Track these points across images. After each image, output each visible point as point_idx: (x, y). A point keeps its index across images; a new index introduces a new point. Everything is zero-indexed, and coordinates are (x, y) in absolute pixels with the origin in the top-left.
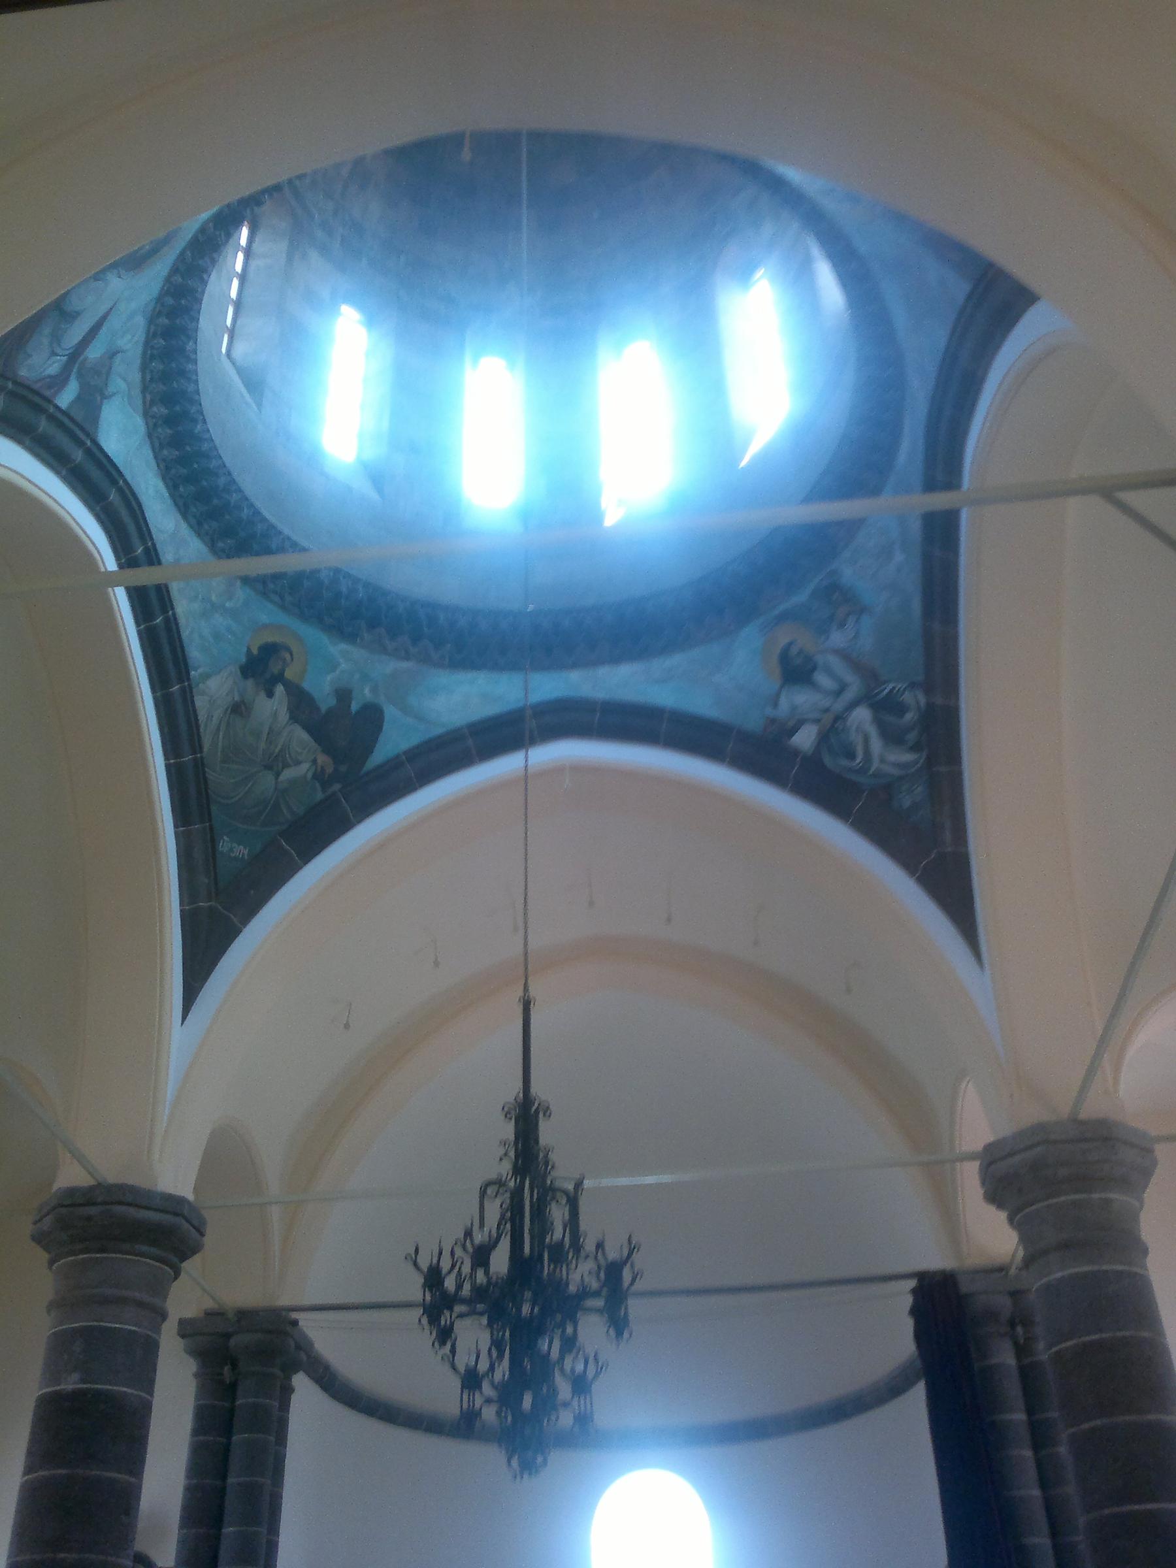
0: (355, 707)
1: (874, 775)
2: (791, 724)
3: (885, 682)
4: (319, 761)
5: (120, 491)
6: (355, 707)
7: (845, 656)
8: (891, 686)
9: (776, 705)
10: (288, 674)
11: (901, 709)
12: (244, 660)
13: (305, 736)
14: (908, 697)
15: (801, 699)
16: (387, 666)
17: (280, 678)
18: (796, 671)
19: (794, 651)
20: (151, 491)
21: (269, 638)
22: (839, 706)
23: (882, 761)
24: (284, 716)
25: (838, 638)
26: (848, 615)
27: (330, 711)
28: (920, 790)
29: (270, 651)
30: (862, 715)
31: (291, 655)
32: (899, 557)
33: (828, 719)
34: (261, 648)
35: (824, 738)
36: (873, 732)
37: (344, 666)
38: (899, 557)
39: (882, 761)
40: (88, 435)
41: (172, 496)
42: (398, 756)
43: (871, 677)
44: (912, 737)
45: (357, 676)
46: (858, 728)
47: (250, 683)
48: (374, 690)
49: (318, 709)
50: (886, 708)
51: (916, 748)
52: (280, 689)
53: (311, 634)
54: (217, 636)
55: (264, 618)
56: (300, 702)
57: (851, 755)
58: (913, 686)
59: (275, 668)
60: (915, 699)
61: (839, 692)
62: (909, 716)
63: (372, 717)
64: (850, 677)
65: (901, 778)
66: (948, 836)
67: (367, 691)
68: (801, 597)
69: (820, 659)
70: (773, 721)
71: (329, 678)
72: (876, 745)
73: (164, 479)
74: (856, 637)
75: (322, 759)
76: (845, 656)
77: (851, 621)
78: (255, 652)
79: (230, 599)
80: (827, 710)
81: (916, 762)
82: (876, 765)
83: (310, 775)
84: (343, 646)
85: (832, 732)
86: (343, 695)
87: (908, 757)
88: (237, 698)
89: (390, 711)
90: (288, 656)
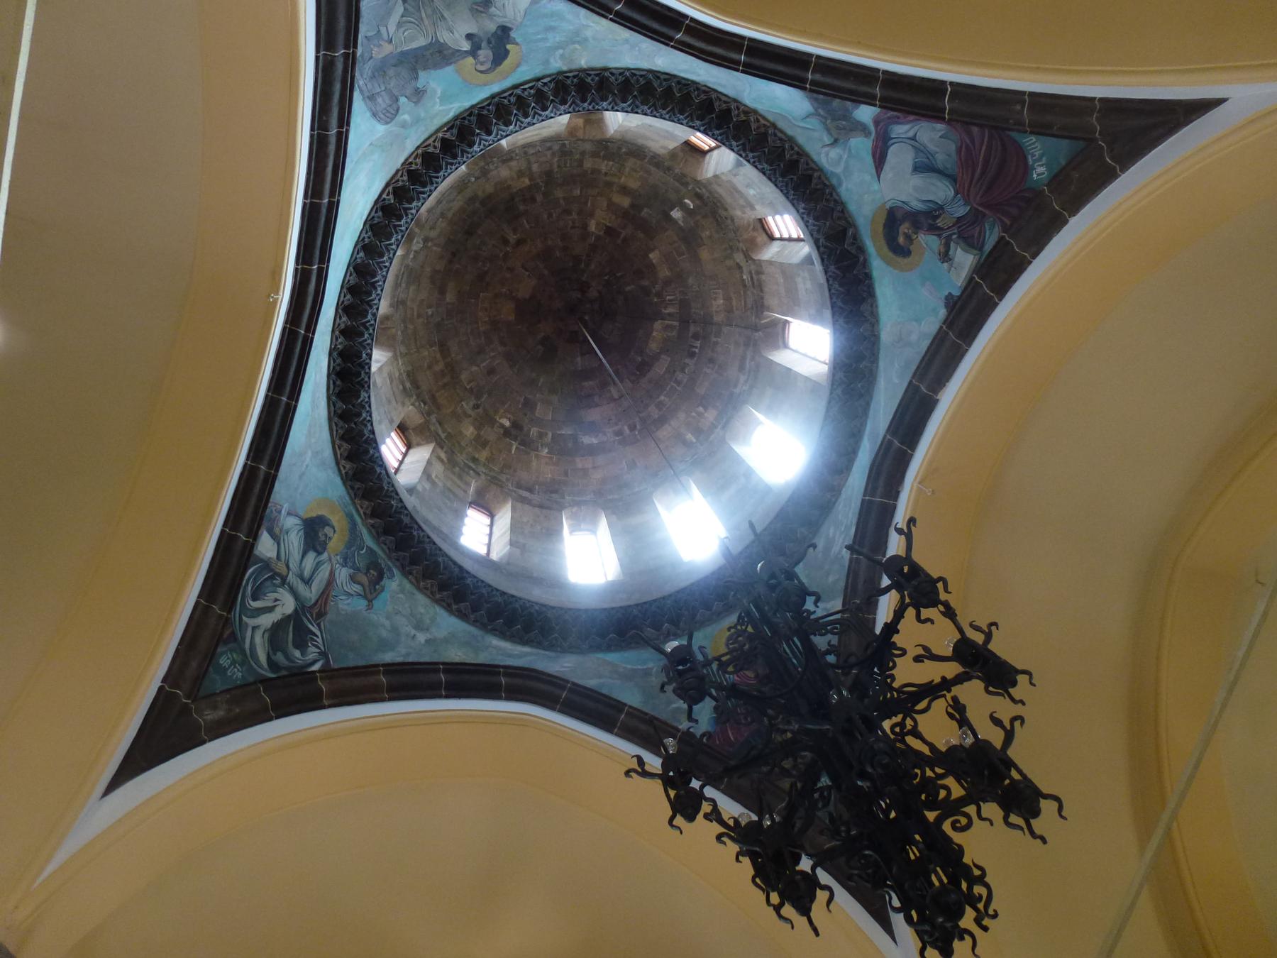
0: (403, 100)
1: (241, 619)
2: (277, 530)
3: (319, 625)
4: (386, 45)
5: (738, 63)
6: (403, 100)
7: (331, 581)
8: (318, 633)
9: (289, 514)
10: (470, 60)
11: (301, 645)
12: (513, 34)
13: (414, 45)
14: (312, 652)
15: (294, 541)
16: (412, 141)
17: (473, 53)
18: (314, 530)
19: (327, 530)
20: (702, 72)
21: (507, 63)
22: (291, 578)
23: (254, 628)
24: (444, 37)
25: (343, 574)
26: (362, 585)
27: (417, 78)
28: (237, 674)
29: (500, 56)
30: (288, 605)
31: (481, 72)
32: (421, 637)
33: (281, 568)
34: (507, 52)
35: (266, 565)
36: (275, 617)
37: (438, 107)
38: (421, 637)
39: (254, 628)
40: (811, 91)
41: (675, 76)
42: (348, 124)
43: (318, 609)
44: (279, 657)
45: (423, 115)
46: (276, 600)
47: (492, 27)
48: (404, 125)
49: (424, 69)
50: (295, 628)
51: (272, 665)
52: (466, 46)
53: (480, 95)
54: (551, 29)
55: (523, 68)
56: (439, 55)
57: (254, 599)
58: (323, 654)
59: (485, 53)
60: (310, 656)
61: (301, 577)
62: (297, 653)
63: (388, 115)
64: (317, 586)
65: (243, 651)
66: (211, 716)
67: (406, 117)
68: (369, 541)
69: (325, 556)
70: (280, 512)
71: (439, 92)
72: (267, 620)
73: (694, 82)
74: (349, 594)
75: (388, 49)
76: (331, 581)
77: (357, 588)
78: (508, 47)
79: (562, 56)
80: (288, 567)
81: (261, 666)
82: (252, 622)
83: (383, 30)
84: (451, 115)
85: (274, 575)
86: (418, 95)
87: (263, 658)
88: (493, 10)
89: (381, 129)
90: (482, 68)
